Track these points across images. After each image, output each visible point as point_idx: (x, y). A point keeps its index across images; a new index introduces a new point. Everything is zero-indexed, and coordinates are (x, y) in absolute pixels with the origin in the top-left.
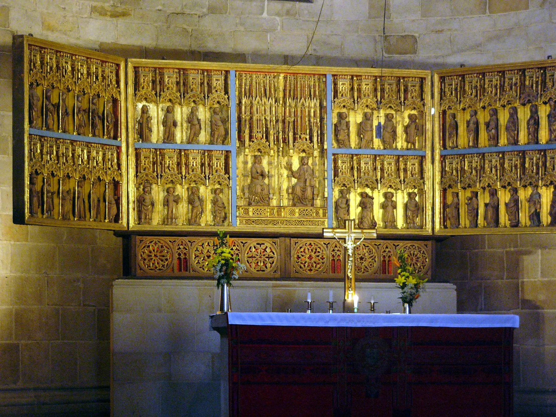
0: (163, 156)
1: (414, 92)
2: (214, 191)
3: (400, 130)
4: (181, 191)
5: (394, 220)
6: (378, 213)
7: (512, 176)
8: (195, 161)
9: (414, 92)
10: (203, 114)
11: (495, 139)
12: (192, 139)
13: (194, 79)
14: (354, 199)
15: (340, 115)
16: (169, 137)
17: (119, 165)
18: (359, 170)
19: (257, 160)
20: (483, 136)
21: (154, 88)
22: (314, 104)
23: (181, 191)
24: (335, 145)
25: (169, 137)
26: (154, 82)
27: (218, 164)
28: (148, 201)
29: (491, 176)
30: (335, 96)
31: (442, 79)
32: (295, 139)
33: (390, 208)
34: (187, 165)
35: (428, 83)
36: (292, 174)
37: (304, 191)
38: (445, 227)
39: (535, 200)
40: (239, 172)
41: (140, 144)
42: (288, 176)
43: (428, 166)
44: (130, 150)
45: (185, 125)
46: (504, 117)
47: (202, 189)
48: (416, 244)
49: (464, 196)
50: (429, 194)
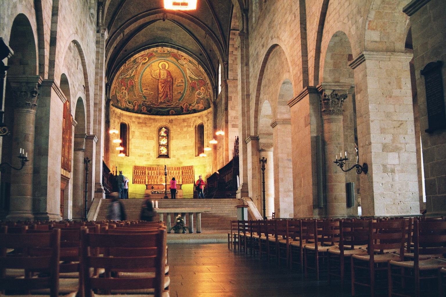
7: (188, 178)
8: (154, 177)
10: (155, 172)
12: (154, 175)
13: (154, 168)
16: (151, 175)
19: (161, 177)
20: (186, 174)
23: (153, 180)
25: (151, 175)
27: (157, 177)
46: (188, 172)
49: (184, 180)
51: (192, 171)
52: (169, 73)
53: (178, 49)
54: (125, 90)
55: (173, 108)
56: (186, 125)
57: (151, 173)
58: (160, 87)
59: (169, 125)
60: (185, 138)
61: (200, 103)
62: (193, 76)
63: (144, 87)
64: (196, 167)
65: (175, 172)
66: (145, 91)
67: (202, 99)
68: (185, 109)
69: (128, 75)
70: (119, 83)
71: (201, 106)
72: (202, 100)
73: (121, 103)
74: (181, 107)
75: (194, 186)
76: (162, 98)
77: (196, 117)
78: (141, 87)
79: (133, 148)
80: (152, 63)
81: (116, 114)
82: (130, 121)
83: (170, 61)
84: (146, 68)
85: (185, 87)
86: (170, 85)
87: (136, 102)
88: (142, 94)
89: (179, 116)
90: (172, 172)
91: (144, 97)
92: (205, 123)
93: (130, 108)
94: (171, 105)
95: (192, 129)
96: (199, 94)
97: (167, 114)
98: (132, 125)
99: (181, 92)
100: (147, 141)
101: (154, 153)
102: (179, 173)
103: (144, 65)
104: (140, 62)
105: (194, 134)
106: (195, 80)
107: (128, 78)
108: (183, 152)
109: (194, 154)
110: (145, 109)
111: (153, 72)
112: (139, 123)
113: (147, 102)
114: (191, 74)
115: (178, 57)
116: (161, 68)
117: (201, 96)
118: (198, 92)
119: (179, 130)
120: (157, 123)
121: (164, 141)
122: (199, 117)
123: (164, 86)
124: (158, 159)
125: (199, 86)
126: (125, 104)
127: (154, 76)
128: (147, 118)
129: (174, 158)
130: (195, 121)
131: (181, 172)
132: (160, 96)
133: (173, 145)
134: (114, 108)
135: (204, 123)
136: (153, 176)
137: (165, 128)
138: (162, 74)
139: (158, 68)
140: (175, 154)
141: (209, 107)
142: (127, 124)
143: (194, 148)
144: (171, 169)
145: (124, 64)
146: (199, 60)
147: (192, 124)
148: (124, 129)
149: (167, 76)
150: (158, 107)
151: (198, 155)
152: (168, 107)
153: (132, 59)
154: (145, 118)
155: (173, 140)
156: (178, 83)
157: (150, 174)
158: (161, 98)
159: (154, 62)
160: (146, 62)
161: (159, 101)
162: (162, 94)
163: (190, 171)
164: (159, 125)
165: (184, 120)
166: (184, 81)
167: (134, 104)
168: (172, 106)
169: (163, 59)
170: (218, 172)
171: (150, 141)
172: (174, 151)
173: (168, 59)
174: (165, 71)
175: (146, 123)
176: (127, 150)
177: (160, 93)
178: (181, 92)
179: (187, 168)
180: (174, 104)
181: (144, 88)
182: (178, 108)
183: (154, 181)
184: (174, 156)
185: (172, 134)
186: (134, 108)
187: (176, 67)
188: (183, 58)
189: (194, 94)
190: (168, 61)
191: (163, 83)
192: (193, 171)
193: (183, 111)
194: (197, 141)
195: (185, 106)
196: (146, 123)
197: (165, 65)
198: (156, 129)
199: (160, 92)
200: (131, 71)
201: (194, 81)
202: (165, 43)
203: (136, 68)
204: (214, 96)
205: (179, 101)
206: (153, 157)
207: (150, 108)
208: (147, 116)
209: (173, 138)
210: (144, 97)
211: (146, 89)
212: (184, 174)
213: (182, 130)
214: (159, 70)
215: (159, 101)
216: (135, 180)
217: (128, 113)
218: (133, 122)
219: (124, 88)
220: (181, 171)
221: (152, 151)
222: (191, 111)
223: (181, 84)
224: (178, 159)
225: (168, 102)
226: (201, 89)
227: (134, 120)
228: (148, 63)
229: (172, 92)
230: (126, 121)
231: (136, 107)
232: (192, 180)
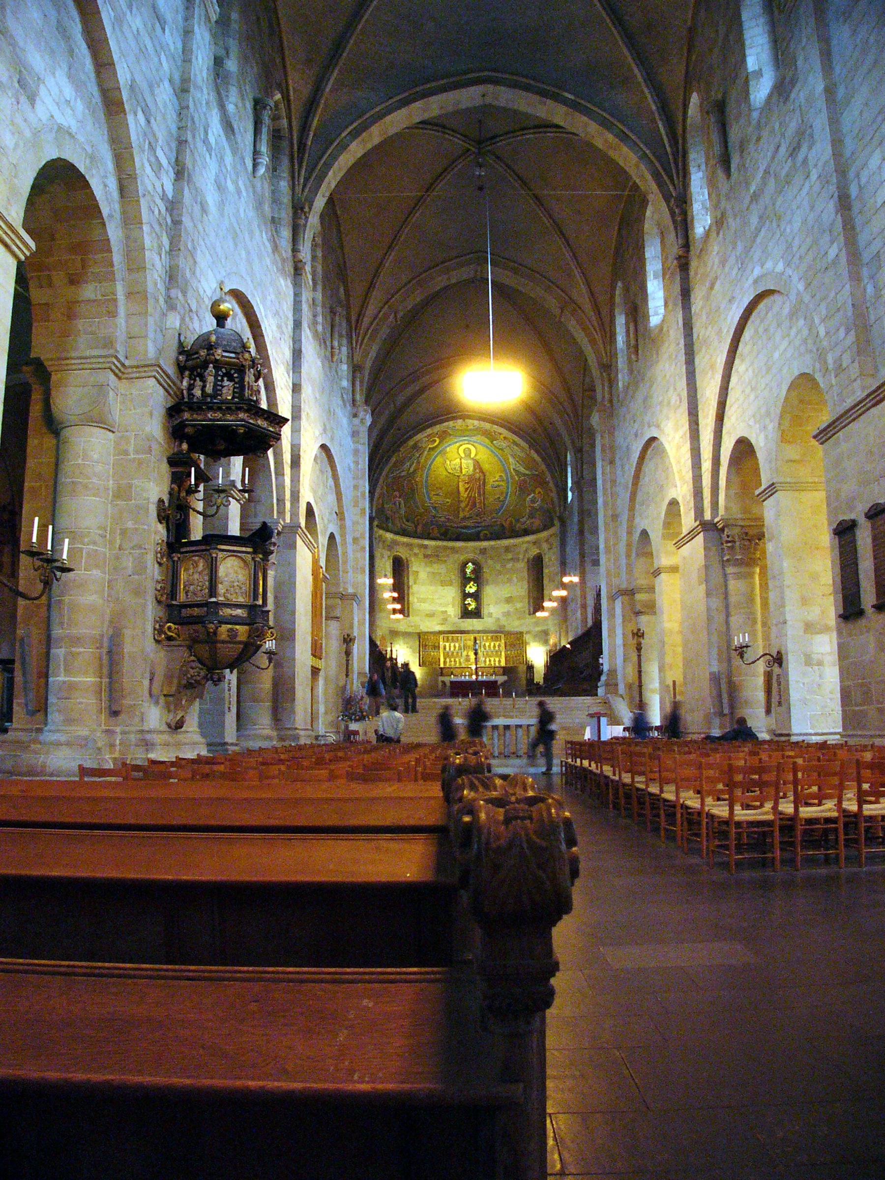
6: (492, 663)
14: (487, 660)
52: (477, 464)
57: (450, 647)
58: (462, 489)
59: (480, 558)
60: (510, 580)
62: (522, 470)
67: (537, 510)
70: (388, 486)
71: (537, 523)
74: (503, 526)
77: (528, 542)
78: (427, 492)
79: (416, 600)
81: (384, 542)
83: (480, 444)
85: (508, 488)
89: (499, 542)
90: (487, 644)
91: (435, 508)
93: (410, 529)
95: (522, 565)
97: (476, 537)
100: (440, 587)
103: (432, 453)
105: (525, 574)
106: (524, 475)
109: (527, 611)
110: (436, 531)
112: (426, 556)
119: (498, 567)
121: (471, 588)
122: (534, 543)
127: (450, 471)
131: (503, 645)
132: (463, 505)
134: (381, 532)
136: (453, 653)
137: (473, 564)
138: (464, 466)
140: (491, 611)
141: (553, 525)
142: (404, 557)
147: (521, 557)
148: (399, 568)
149: (475, 469)
151: (534, 613)
153: (411, 443)
155: (487, 583)
157: (447, 649)
158: (463, 510)
160: (436, 447)
161: (461, 515)
164: (462, 558)
165: (507, 549)
168: (483, 524)
170: (568, 646)
173: (474, 439)
174: (471, 462)
175: (437, 556)
180: (488, 520)
183: (455, 661)
195: (508, 522)
197: (470, 450)
208: (439, 543)
210: (435, 508)
212: (508, 648)
213: (503, 566)
215: (461, 515)
217: (405, 540)
218: (415, 554)
220: (503, 641)
221: (451, 606)
223: (501, 483)
227: (416, 550)
230: (403, 553)
231: (419, 529)
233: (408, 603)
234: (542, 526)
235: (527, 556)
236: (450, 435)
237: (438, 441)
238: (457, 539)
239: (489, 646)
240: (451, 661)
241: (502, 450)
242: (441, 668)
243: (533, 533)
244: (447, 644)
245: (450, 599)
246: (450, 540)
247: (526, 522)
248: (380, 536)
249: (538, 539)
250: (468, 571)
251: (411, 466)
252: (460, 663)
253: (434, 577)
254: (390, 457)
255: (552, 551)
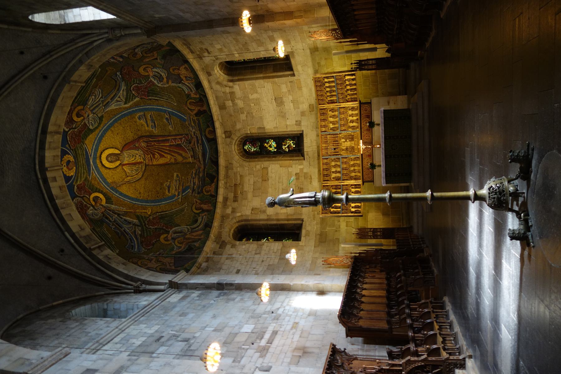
0: (344, 174)
1: (323, 111)
2: (352, 161)
3: (333, 114)
4: (352, 169)
5: (356, 114)
6: (355, 118)
7: (343, 87)
8: (345, 166)
9: (323, 111)
10: (333, 164)
11: (334, 91)
12: (339, 166)
13: (325, 167)
14: (351, 125)
15: (331, 130)
16: (339, 172)
17: (347, 185)
18: (344, 124)
20: (334, 94)
21: (328, 176)
22: (328, 136)
23: (352, 169)
24: (338, 130)
25: (339, 172)
26: (327, 176)
27: (345, 160)
28: (355, 177)
29: (344, 91)
30: (326, 131)
31: (320, 104)
32: (337, 141)
33: (353, 115)
34: (346, 168)
35: (321, 108)
36: (346, 141)
37: (350, 138)
38: (357, 101)
39: (349, 80)
40: (346, 155)
41: (342, 179)
42: (347, 142)
43: (341, 106)
44: (343, 182)
45: (336, 168)
46: (328, 89)
47: (351, 164)
48: (362, 109)
49: (349, 97)
50: (349, 105)
51: (326, 80)
52: (127, 146)
53: (44, 132)
54: (168, 232)
55: (200, 130)
56: (230, 102)
57: (336, 172)
58: (162, 161)
59: (236, 137)
60: (257, 102)
61: (179, 75)
62: (122, 93)
63: (164, 193)
64: (316, 72)
65: (331, 119)
66: (173, 191)
68: (199, 108)
69: (135, 231)
71: (183, 72)
72: (171, 70)
73: (194, 242)
74: (196, 115)
75: (365, 70)
76: (184, 154)
77: (209, 82)
78: (165, 200)
80: (107, 183)
82: (232, 219)
84: (121, 194)
86: (155, 141)
87: (194, 208)
88: (178, 195)
89: (215, 118)
90: (331, 126)
91: (184, 191)
92: (217, 59)
94: (197, 137)
95: (237, 88)
96: (160, 79)
97: (213, 141)
98: (238, 214)
99: (167, 118)
100: (269, 181)
101: (294, 166)
102: (332, 110)
104: (103, 210)
105: (247, 83)
106: (128, 90)
107: (142, 231)
108: (289, 106)
110: (208, 188)
111: (129, 178)
112: (235, 200)
113: (194, 184)
114: (119, 99)
115: (80, 132)
116: (118, 163)
117: (163, 74)
118: (155, 82)
119: (243, 117)
120: (234, 163)
122: (209, 74)
123: (158, 153)
124: (306, 156)
125: (140, 81)
126: (197, 231)
127: (140, 175)
128: (226, 183)
129: (302, 124)
130: (218, 83)
131: (332, 106)
132: (180, 159)
133: (274, 128)
135: (219, 62)
136: (343, 169)
137: (245, 144)
138: (132, 160)
139: (120, 167)
140: (295, 123)
142: (237, 225)
143: (276, 79)
144: (324, 129)
145: (94, 252)
146: (58, 81)
149: (137, 148)
150: (202, 163)
152: (200, 142)
154: (226, 188)
155: (264, 128)
156: (148, 126)
157: (338, 175)
158: (184, 158)
159: (105, 180)
160: (105, 195)
161: (190, 160)
162: (176, 155)
163: (327, 85)
164: (236, 158)
165: (222, 107)
166: (142, 113)
167: (197, 212)
168: (199, 136)
169: (95, 163)
171: (270, 174)
172: (288, 123)
174: (125, 154)
176: (290, 222)
177: (175, 159)
178: (167, 118)
179: (319, 93)
181: (167, 193)
182: (199, 121)
184: (298, 123)
185: (252, 130)
186: (208, 211)
187: (109, 133)
188: (75, 118)
189: (162, 89)
190: (96, 150)
191: (154, 155)
192: (327, 78)
193: (205, 111)
194: (262, 75)
196: (235, 185)
197: (110, 155)
198: (246, 164)
199: (173, 161)
200: (125, 227)
201: (134, 93)
202: (35, 164)
203: (119, 215)
204: (135, 35)
205: (185, 120)
206: (301, 167)
207: (207, 179)
208: (221, 184)
209: (260, 128)
210: (183, 191)
211: (169, 187)
212: (334, 98)
213: (241, 111)
214: (123, 167)
215: (190, 160)
216: (353, 210)
217: (216, 224)
218: (234, 211)
219: (162, 237)
221: (290, 169)
222: (200, 95)
224: (303, 114)
225: (190, 143)
226: (147, 74)
227: (229, 211)
228: (108, 190)
229: (169, 136)
231: (205, 207)
232: (347, 77)
233: (288, 220)
234: (186, 65)
235: (225, 83)
236: (86, 179)
237: (97, 194)
238: (216, 163)
239: (333, 123)
240: (354, 171)
241: (101, 119)
242: (363, 183)
243: (196, 77)
244: (334, 175)
245: (283, 171)
246: (217, 172)
247: (187, 87)
248: (208, 260)
249: (203, 69)
250: (253, 149)
251: (129, 223)
252: (356, 159)
253: (260, 191)
254: (100, 262)
255: (210, 49)
